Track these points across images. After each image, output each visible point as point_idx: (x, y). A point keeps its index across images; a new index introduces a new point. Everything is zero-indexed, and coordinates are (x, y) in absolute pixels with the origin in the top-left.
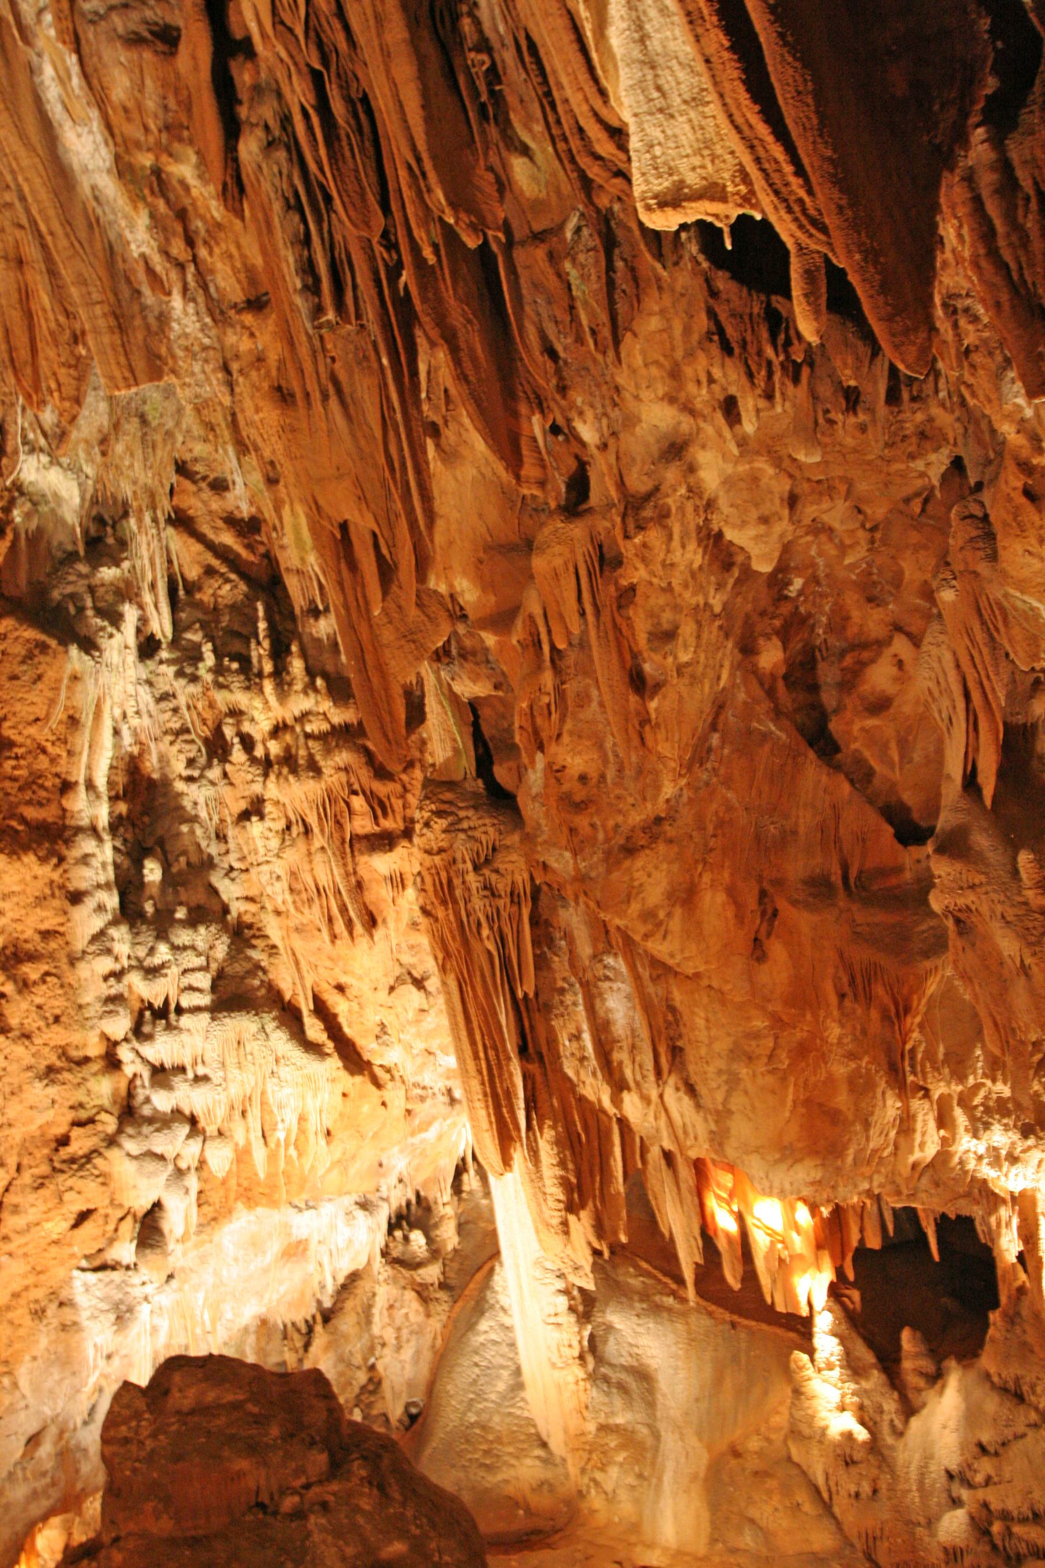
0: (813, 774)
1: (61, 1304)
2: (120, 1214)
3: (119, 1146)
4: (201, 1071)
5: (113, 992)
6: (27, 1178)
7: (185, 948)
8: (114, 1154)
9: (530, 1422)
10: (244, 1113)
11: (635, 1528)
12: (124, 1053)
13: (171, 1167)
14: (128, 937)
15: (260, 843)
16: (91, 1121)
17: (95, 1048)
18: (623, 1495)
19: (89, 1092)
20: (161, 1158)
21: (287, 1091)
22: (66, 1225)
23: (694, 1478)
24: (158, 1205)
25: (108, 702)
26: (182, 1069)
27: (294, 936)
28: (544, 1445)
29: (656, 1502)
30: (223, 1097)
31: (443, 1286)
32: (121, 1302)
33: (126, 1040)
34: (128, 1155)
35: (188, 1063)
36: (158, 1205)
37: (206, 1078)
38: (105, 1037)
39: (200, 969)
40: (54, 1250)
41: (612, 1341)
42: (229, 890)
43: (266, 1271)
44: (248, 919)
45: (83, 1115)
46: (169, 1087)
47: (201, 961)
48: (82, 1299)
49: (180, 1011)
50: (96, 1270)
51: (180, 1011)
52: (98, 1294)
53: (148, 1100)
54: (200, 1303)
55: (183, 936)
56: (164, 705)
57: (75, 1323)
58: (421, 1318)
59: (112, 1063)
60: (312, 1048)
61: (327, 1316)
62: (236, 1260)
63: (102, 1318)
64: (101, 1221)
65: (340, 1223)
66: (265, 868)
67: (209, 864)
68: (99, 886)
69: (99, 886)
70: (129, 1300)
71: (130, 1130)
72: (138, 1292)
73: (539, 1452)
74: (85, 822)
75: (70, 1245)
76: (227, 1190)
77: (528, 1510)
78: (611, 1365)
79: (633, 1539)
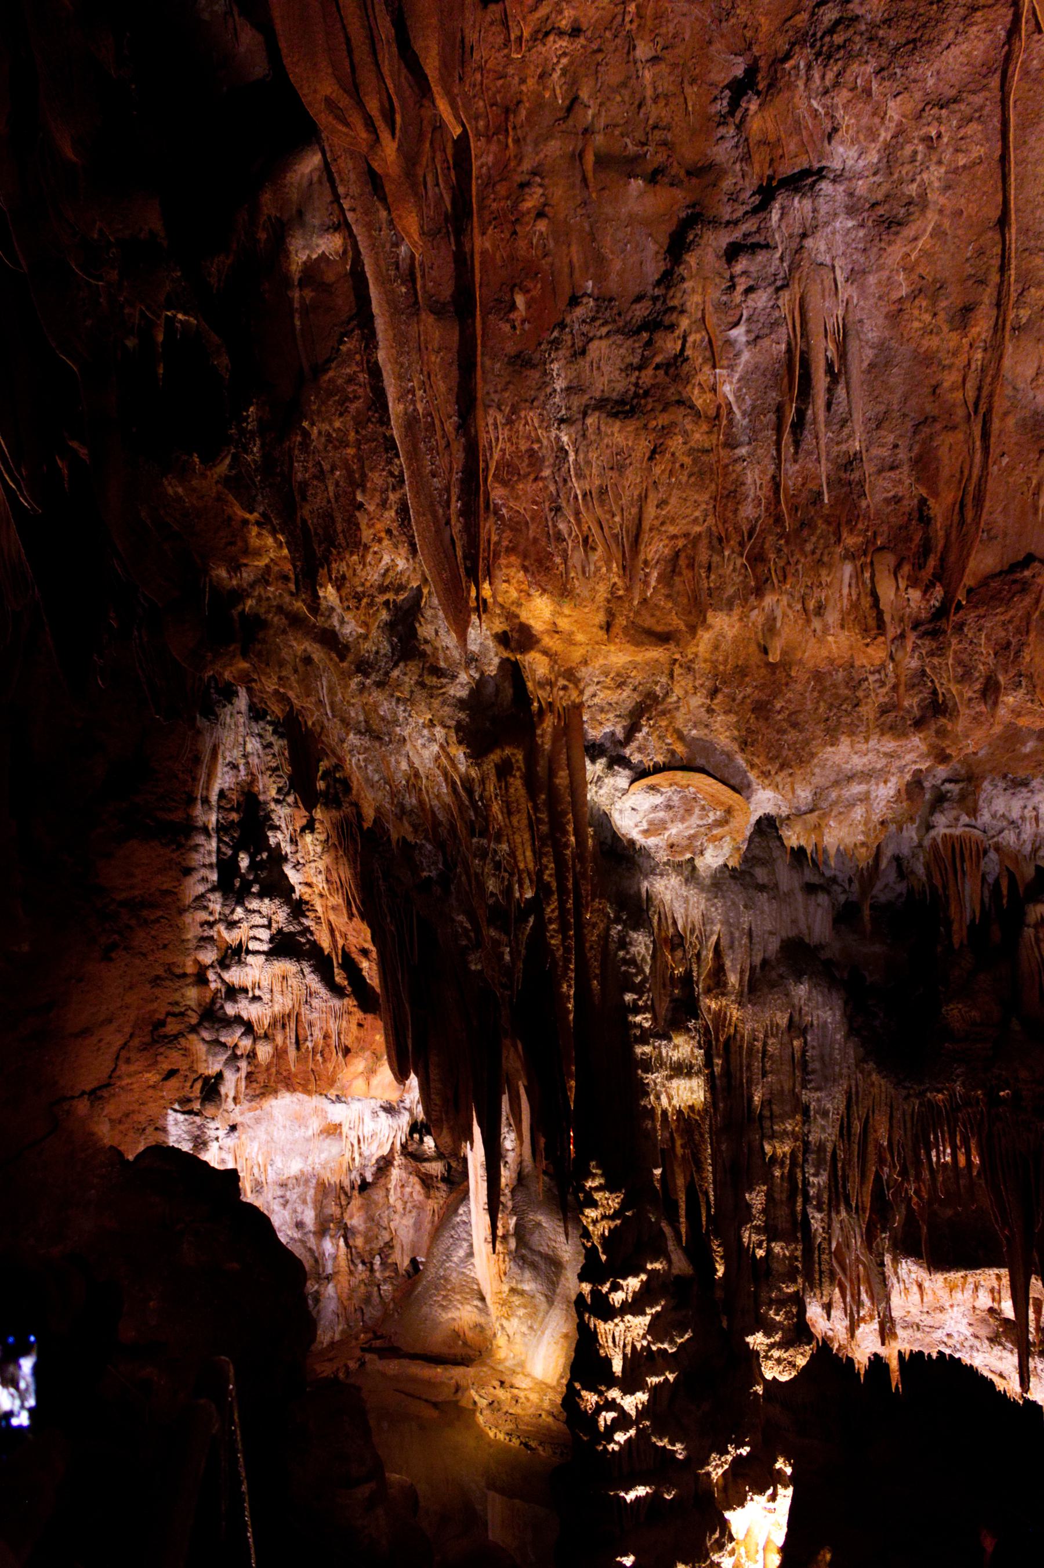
1: (157, 1129)
2: (195, 1076)
3: (198, 1033)
4: (257, 993)
5: (206, 934)
6: (136, 1042)
7: (254, 911)
8: (193, 1037)
9: (475, 1281)
10: (284, 1026)
11: (522, 1365)
12: (211, 976)
13: (229, 1052)
14: (220, 900)
15: (311, 848)
16: (182, 1014)
17: (190, 969)
18: (518, 1338)
19: (183, 996)
20: (224, 1045)
21: (315, 1015)
22: (158, 1077)
23: (566, 1336)
24: (220, 1076)
25: (222, 747)
26: (245, 990)
27: (331, 912)
28: (483, 1299)
29: (537, 1346)
30: (269, 1012)
31: (444, 1179)
32: (198, 1137)
34: (203, 1039)
35: (249, 985)
36: (220, 1076)
37: (259, 998)
38: (197, 962)
39: (263, 926)
40: (150, 1092)
41: (536, 1235)
42: (294, 877)
43: (308, 1140)
44: (306, 897)
45: (177, 1010)
46: (235, 1001)
47: (265, 921)
49: (248, 952)
50: (184, 1113)
51: (248, 952)
53: (222, 1007)
54: (256, 1149)
55: (254, 904)
56: (268, 750)
58: (421, 1198)
59: (201, 980)
60: (337, 991)
61: (364, 1186)
62: (284, 1127)
64: (182, 1079)
65: (367, 1118)
66: (313, 865)
67: (285, 859)
68: (204, 866)
69: (204, 866)
71: (206, 1025)
72: (212, 1133)
73: (477, 1303)
74: (200, 824)
76: (270, 1075)
77: (465, 1343)
78: (531, 1249)
79: (519, 1370)
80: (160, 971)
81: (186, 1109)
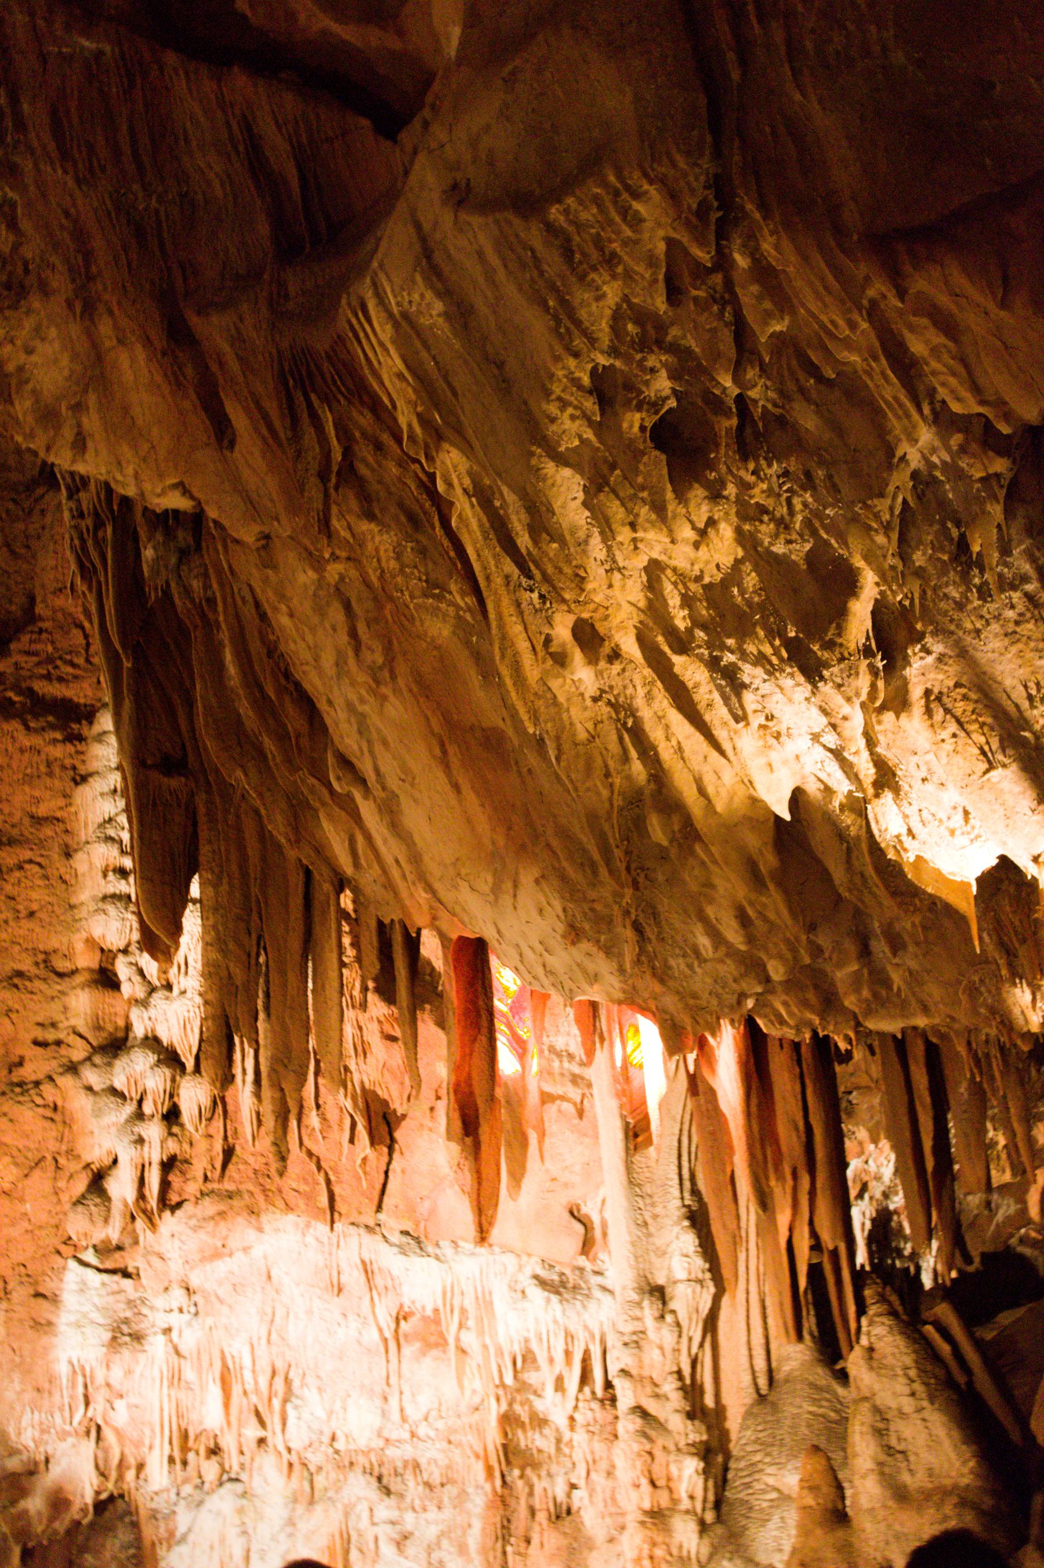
0: (196, 100)
1: (38, 1295)
12: (122, 969)
17: (86, 960)
32: (126, 1321)
33: (125, 951)
34: (89, 1088)
45: (51, 1036)
48: (70, 1298)
52: (96, 1300)
57: (50, 1323)
63: (88, 1330)
70: (143, 1326)
75: (22, 1200)
80: (26, 965)
81: (109, 1265)
